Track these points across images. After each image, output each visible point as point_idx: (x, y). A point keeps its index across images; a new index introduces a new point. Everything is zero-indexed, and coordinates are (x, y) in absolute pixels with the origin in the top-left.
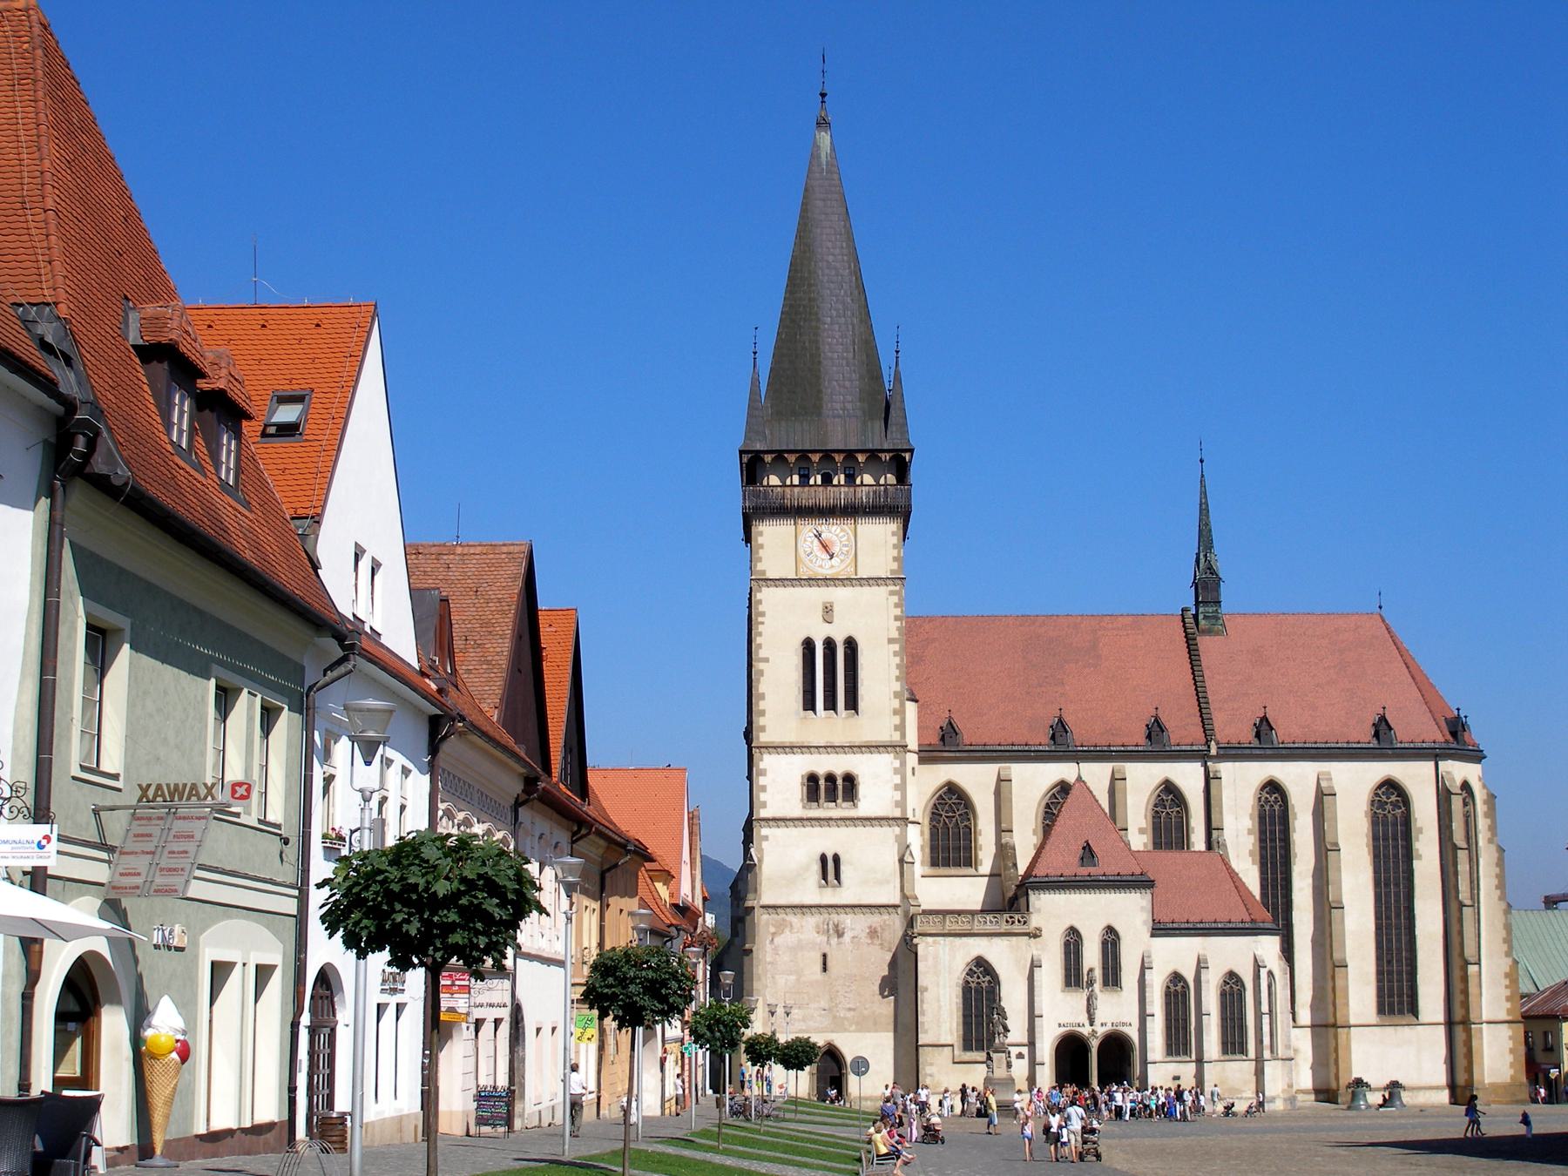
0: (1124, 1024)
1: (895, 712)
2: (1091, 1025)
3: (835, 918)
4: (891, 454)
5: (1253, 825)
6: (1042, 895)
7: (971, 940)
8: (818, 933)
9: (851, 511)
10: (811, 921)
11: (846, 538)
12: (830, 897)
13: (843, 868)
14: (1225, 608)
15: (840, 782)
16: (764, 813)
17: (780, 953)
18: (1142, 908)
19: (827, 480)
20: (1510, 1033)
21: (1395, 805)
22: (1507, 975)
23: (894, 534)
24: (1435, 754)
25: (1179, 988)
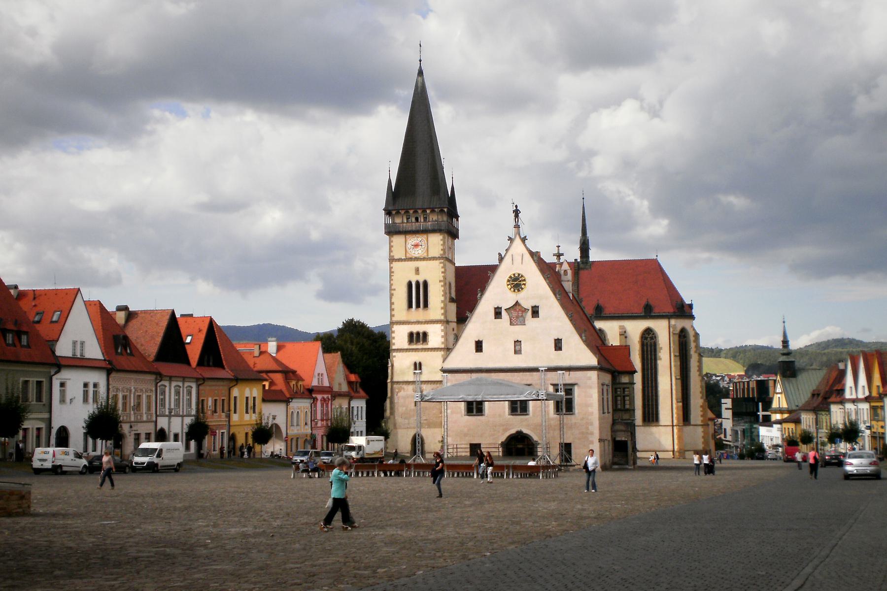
1: (442, 308)
4: (439, 209)
9: (426, 231)
10: (411, 387)
13: (422, 367)
14: (591, 260)
16: (394, 347)
19: (417, 219)
20: (702, 430)
22: (701, 406)
24: (668, 317)
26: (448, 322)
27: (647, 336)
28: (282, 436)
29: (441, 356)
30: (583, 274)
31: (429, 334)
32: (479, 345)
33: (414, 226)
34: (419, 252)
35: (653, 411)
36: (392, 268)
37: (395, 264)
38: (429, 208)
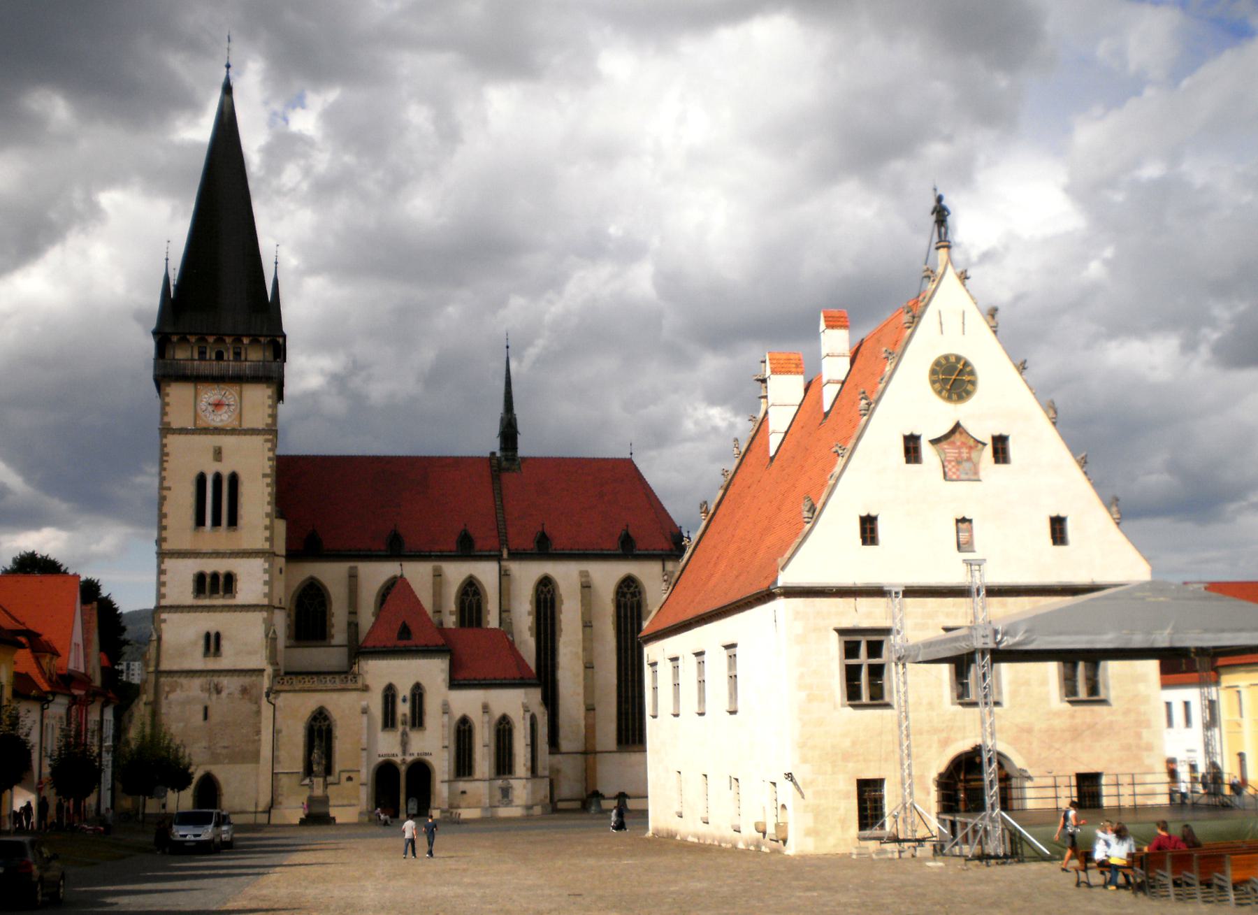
0: (426, 754)
1: (266, 528)
2: (404, 752)
3: (216, 679)
4: (269, 339)
5: (532, 609)
8: (202, 691)
9: (239, 379)
10: (197, 682)
11: (232, 399)
12: (212, 664)
13: (224, 644)
15: (222, 579)
16: (164, 602)
17: (173, 706)
18: (442, 671)
19: (220, 356)
21: (633, 595)
23: (269, 397)
25: (467, 728)
26: (275, 554)
27: (632, 590)
28: (33, 781)
29: (261, 620)
30: (507, 477)
31: (238, 578)
32: (868, 526)
33: (211, 367)
34: (222, 418)
35: (634, 725)
36: (165, 445)
37: (171, 440)
38: (247, 336)
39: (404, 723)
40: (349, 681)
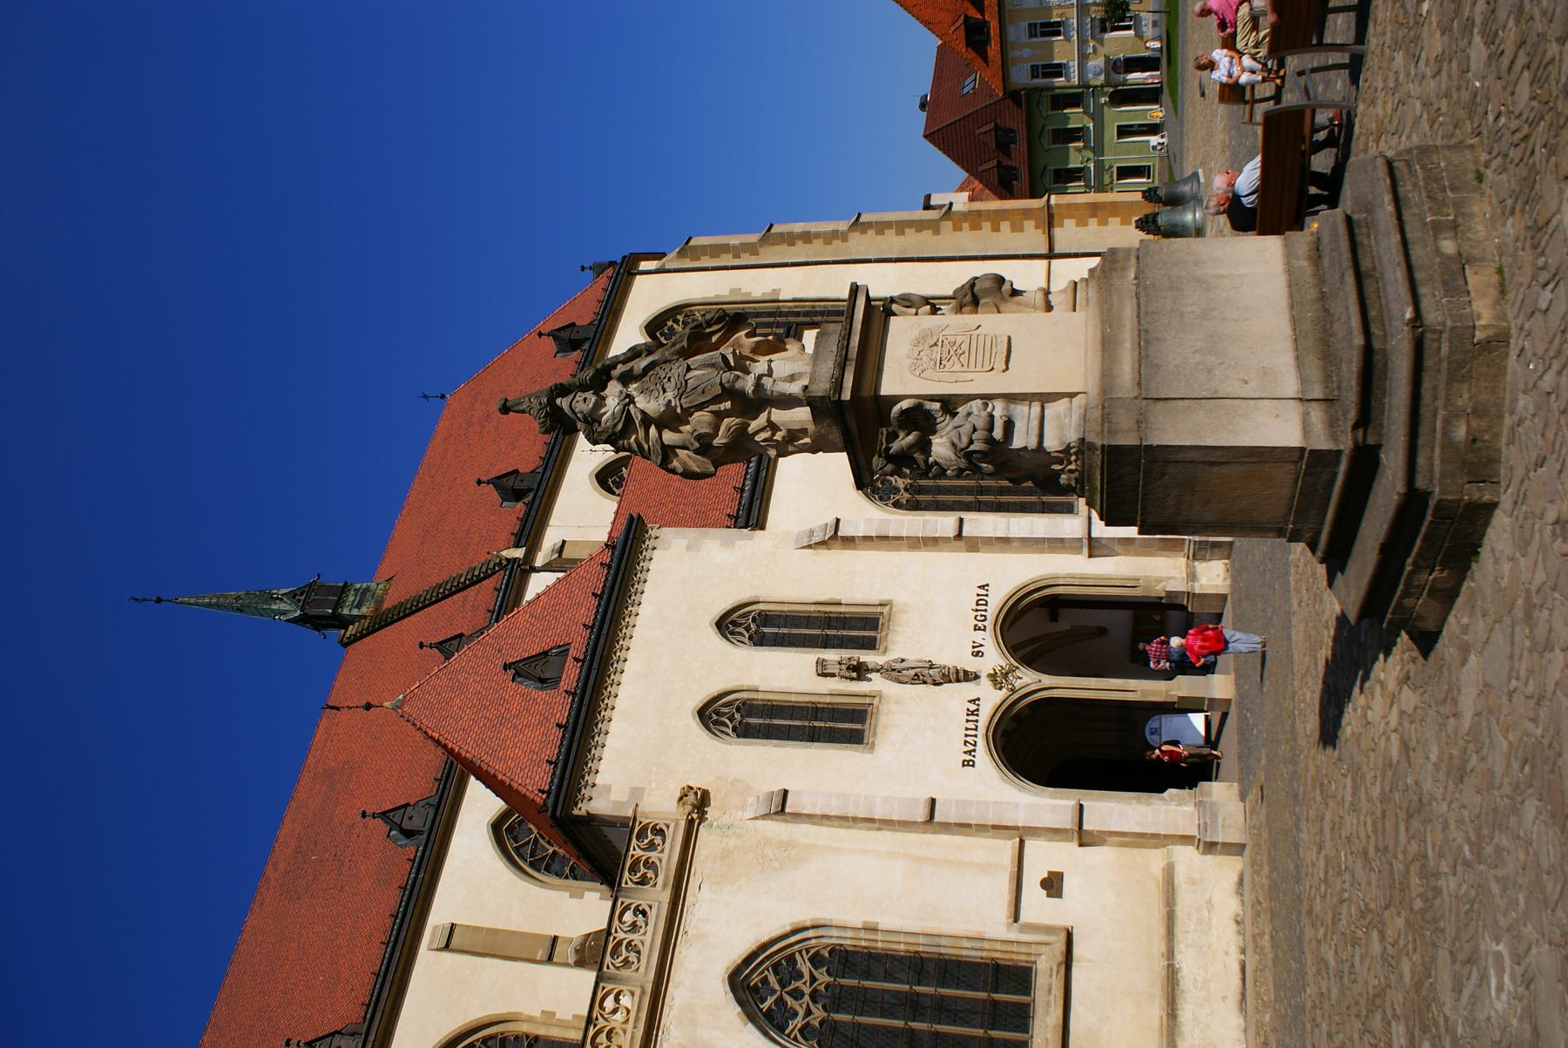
0: (981, 602)
2: (968, 677)
6: (600, 780)
7: (677, 995)
39: (859, 671)
40: (653, 855)
